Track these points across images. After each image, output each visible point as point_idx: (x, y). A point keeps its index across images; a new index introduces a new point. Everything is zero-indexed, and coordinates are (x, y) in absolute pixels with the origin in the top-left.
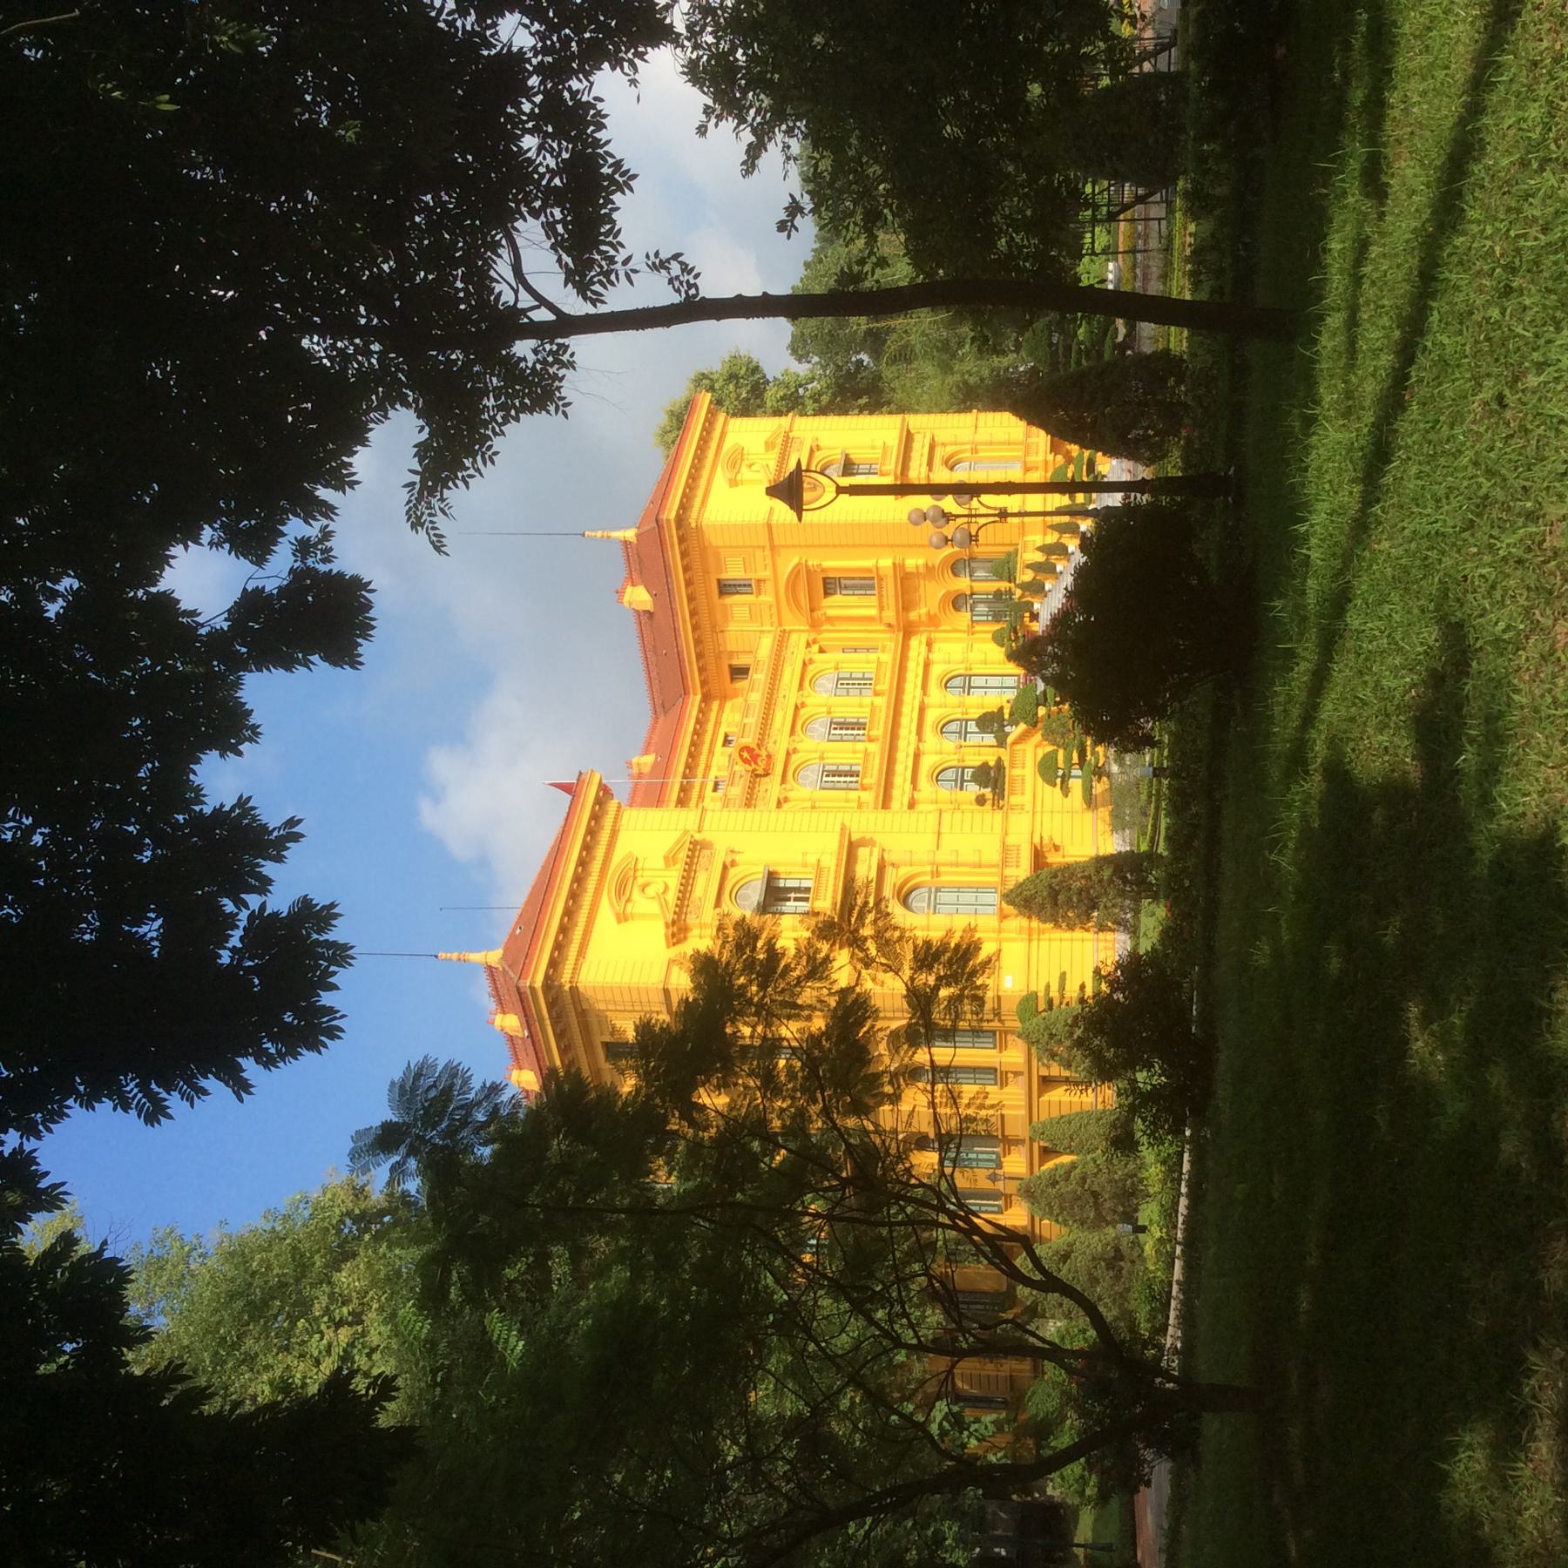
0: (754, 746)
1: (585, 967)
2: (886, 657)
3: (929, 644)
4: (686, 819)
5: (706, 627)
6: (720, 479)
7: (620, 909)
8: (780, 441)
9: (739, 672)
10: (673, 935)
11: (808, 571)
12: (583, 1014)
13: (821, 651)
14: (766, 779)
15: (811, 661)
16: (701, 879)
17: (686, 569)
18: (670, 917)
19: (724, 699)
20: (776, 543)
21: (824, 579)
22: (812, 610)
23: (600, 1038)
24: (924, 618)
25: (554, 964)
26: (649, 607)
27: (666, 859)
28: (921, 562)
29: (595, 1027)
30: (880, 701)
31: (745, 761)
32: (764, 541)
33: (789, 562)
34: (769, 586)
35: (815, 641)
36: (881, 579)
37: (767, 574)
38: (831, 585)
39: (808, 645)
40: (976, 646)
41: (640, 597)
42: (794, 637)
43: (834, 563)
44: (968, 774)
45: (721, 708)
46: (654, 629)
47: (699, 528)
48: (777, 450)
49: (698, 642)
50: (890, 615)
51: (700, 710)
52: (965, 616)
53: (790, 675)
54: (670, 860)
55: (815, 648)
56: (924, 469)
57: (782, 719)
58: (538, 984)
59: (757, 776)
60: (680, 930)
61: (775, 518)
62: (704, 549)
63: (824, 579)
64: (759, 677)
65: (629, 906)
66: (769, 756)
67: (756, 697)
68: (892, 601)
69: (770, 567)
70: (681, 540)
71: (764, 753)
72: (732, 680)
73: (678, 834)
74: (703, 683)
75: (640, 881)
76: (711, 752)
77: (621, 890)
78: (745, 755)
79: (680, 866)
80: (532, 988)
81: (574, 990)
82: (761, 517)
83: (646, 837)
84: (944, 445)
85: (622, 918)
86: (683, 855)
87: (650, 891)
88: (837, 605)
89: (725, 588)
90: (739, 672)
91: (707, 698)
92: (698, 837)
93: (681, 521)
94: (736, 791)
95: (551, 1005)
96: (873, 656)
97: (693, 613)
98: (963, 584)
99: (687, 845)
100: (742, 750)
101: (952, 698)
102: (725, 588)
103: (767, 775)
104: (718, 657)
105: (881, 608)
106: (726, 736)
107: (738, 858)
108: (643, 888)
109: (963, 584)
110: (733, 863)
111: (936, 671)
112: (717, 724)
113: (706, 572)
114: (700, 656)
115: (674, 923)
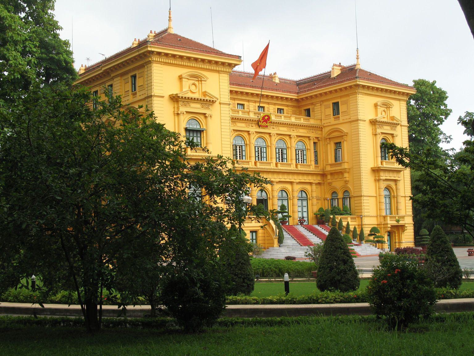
0: (270, 121)
1: (159, 65)
2: (312, 168)
3: (319, 184)
4: (225, 97)
5: (323, 98)
6: (379, 100)
7: (184, 76)
8: (395, 122)
9: (308, 113)
10: (174, 97)
11: (342, 136)
12: (142, 66)
13: (314, 143)
14: (257, 126)
15: (310, 139)
16: (198, 106)
17: (341, 89)
18: (180, 95)
19: (299, 107)
20: (352, 123)
21: (341, 142)
22: (329, 138)
23: (136, 72)
24: (328, 181)
25: (159, 54)
26: (332, 76)
27: (205, 92)
28: (347, 179)
29: (141, 71)
30: (293, 168)
31: (263, 118)
32: (353, 118)
33: (345, 128)
34: (337, 122)
35: (319, 140)
36: (341, 163)
37: (341, 121)
38: (338, 145)
39: (318, 138)
40: (320, 201)
41: (336, 73)
42: (320, 132)
43: (345, 146)
44: (285, 203)
45: (293, 106)
46: (324, 79)
47: (355, 93)
48: (391, 121)
49: (316, 96)
50: (329, 168)
51: (291, 99)
52: (329, 197)
53: (302, 132)
54: (205, 94)
55: (316, 141)
56: (384, 178)
57: (283, 130)
58: (149, 49)
59: (258, 124)
60: (177, 99)
61: (361, 122)
62: (348, 95)
63: (341, 142)
64: (302, 121)
65: (186, 80)
66: (267, 126)
67: (293, 120)
68: (334, 169)
69: (344, 121)
70: (351, 87)
71: (268, 124)
72: (305, 110)
73: (218, 96)
74: (302, 99)
75: (197, 83)
76: (275, 104)
77: (193, 76)
78: (266, 118)
79: (203, 98)
80: (147, 47)
81: (150, 62)
82: (361, 117)
83: (217, 85)
84: (396, 184)
85: (181, 78)
86: (208, 98)
87: (193, 88)
88: (331, 148)
89: (336, 106)
90: (308, 113)
91: (297, 100)
92: (217, 102)
93: (358, 86)
94: (252, 116)
95: (143, 53)
96: (313, 163)
97: (326, 93)
98: (340, 196)
99: (212, 99)
100: (268, 116)
101: (297, 194)
102: (336, 106)
103: (259, 126)
104: (312, 104)
105: (331, 165)
106: (283, 109)
107: (209, 119)
108: (194, 84)
109: (340, 196)
110: (206, 117)
111: (308, 187)
112: (287, 106)
113: (341, 97)
114: (311, 97)
115: (179, 97)
